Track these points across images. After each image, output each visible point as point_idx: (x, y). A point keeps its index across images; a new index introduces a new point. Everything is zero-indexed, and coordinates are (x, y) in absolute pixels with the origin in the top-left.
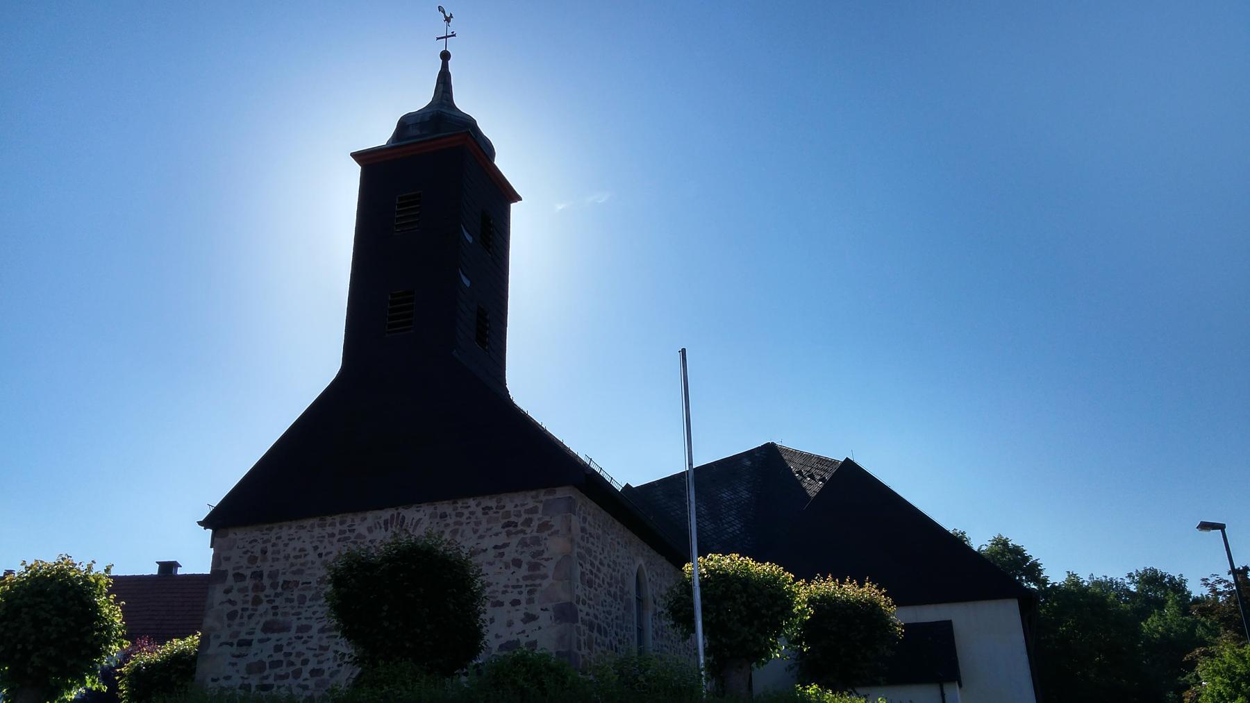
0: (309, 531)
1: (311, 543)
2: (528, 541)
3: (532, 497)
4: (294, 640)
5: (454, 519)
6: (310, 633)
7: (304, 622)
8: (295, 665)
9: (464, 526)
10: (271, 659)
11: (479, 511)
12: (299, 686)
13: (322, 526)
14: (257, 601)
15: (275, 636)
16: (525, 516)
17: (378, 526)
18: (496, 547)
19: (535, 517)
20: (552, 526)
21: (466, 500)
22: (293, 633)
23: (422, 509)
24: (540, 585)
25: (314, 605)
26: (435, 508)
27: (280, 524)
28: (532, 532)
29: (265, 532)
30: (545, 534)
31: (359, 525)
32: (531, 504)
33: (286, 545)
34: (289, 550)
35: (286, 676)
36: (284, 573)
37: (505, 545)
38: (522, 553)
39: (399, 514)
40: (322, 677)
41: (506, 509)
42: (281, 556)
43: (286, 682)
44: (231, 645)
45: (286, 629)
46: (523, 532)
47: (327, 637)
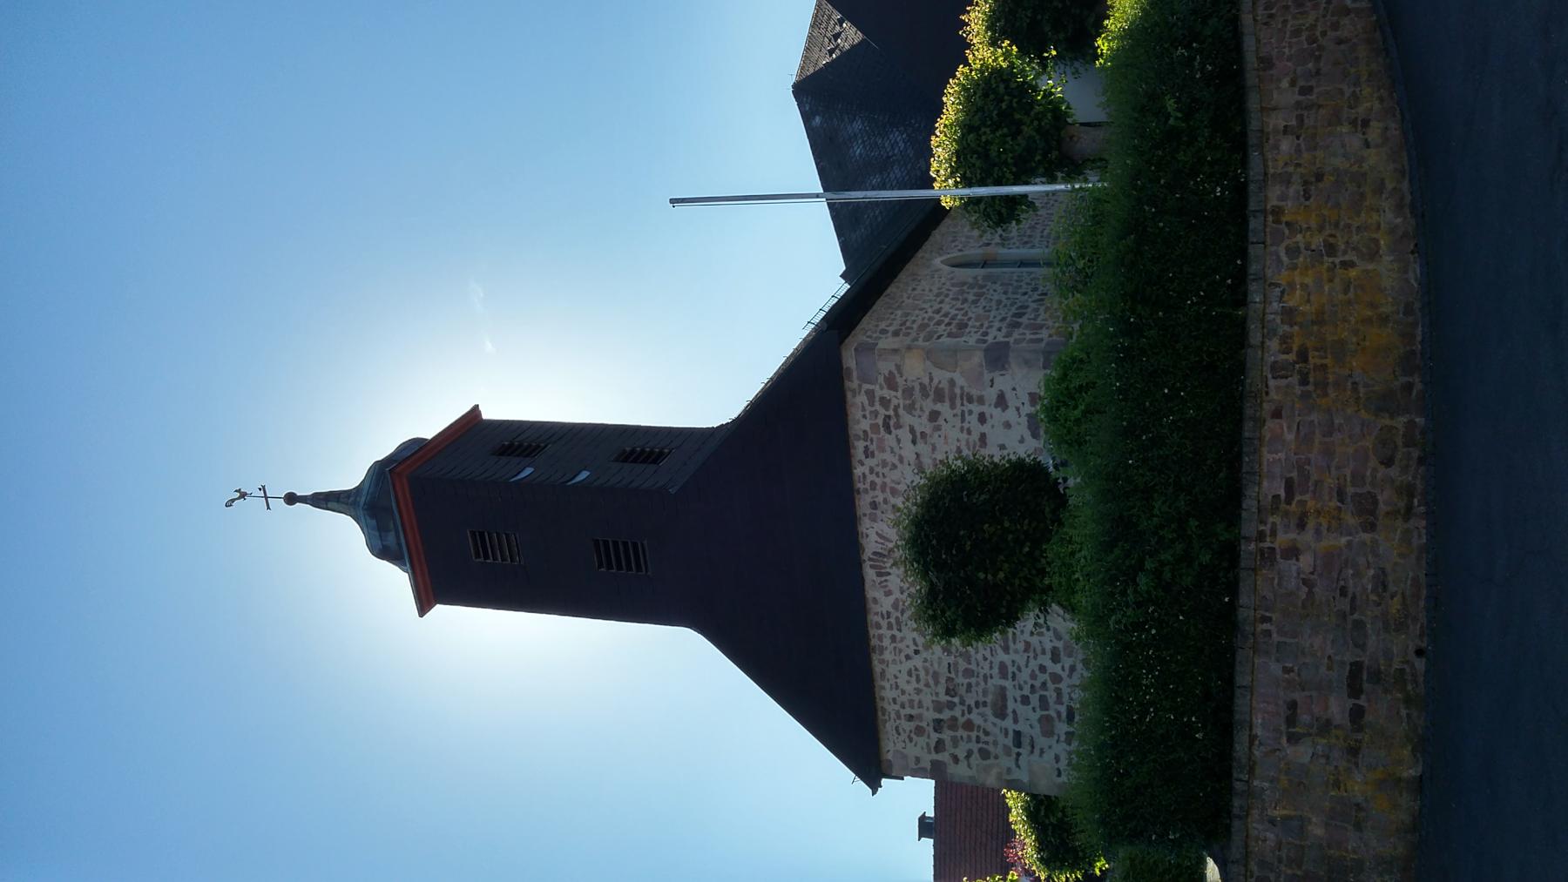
0: (887, 666)
1: (901, 663)
2: (908, 402)
3: (854, 396)
4: (1016, 682)
5: (878, 492)
6: (1009, 663)
7: (996, 671)
8: (1046, 680)
9: (887, 480)
10: (1038, 710)
11: (870, 462)
12: (1070, 676)
13: (882, 650)
14: (969, 726)
15: (1011, 705)
16: (878, 407)
17: (885, 584)
18: (914, 442)
19: (879, 393)
20: (890, 372)
21: (856, 478)
22: (1008, 684)
23: (865, 531)
24: (962, 388)
25: (976, 659)
26: (865, 515)
27: (878, 700)
28: (896, 397)
29: (887, 717)
30: (900, 381)
31: (882, 606)
32: (862, 399)
33: (903, 692)
34: (909, 688)
35: (1059, 692)
36: (937, 694)
37: (912, 430)
38: (922, 409)
39: (870, 559)
40: (1061, 649)
41: (868, 429)
42: (916, 698)
43: (1065, 691)
44: (1019, 754)
45: (1003, 689)
46: (896, 408)
47: (1014, 643)
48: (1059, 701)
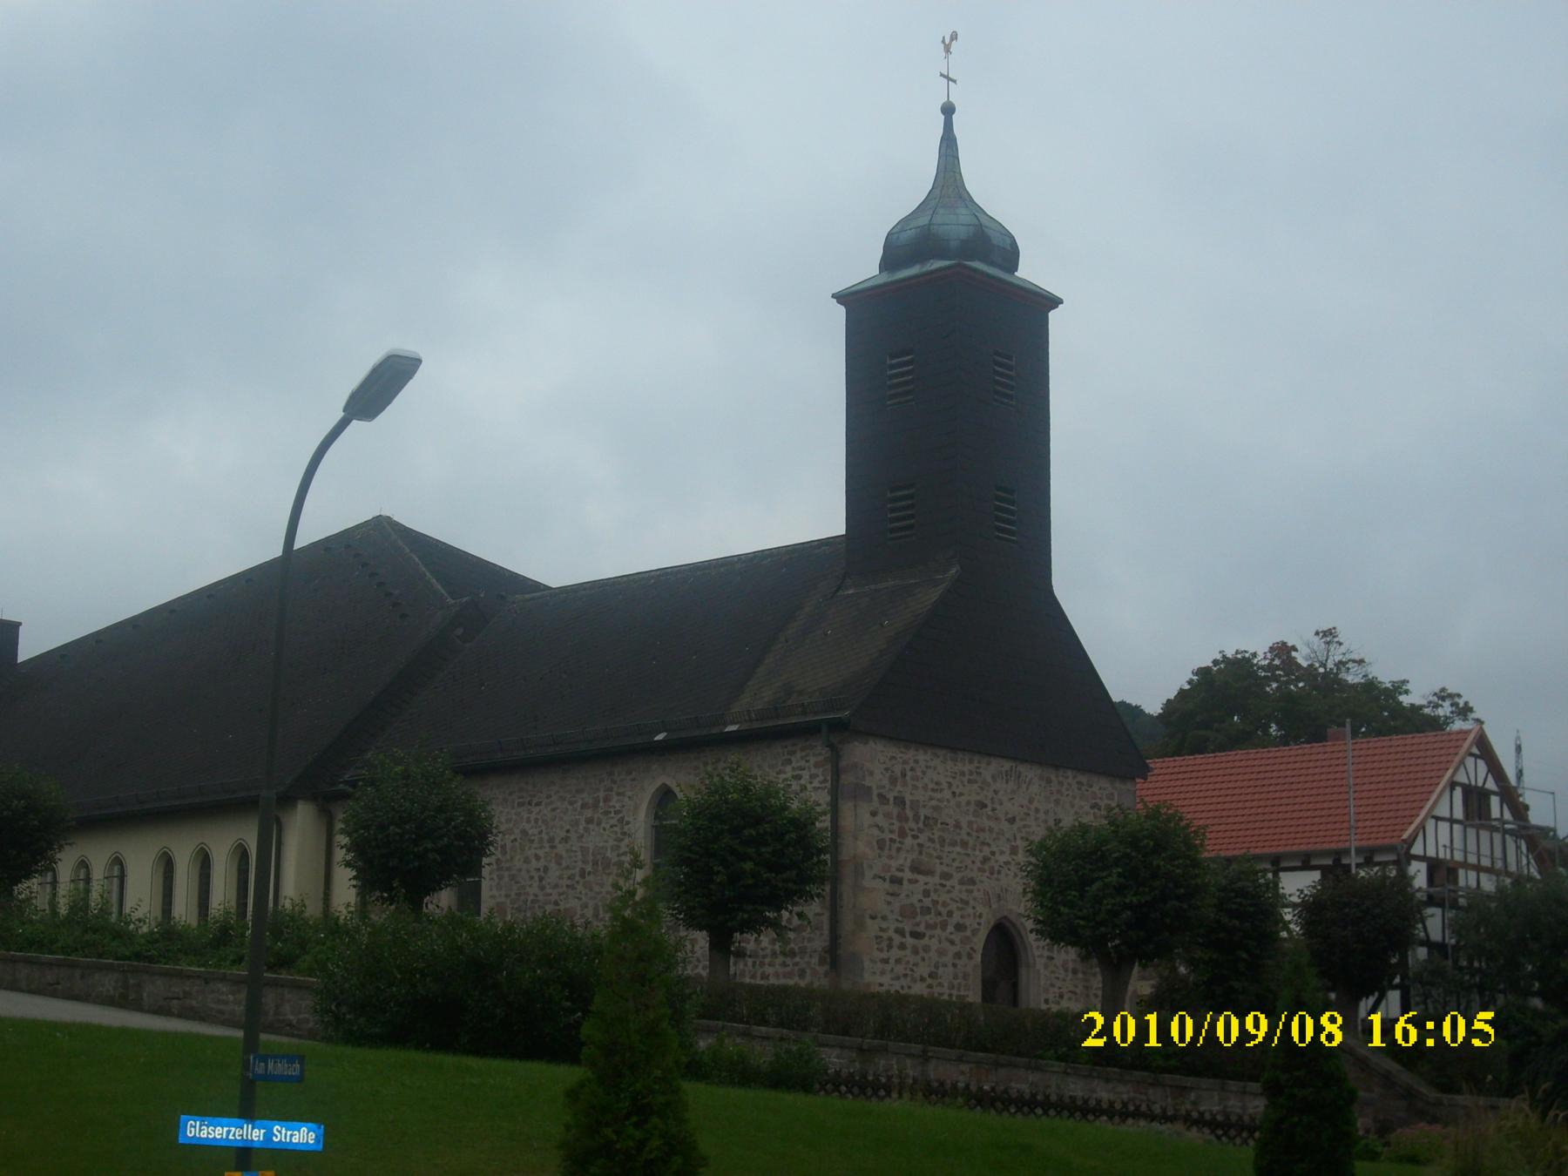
7: (945, 869)
14: (902, 834)
15: (922, 878)
35: (933, 927)
36: (924, 806)
44: (884, 880)
45: (930, 873)
48: (928, 926)
